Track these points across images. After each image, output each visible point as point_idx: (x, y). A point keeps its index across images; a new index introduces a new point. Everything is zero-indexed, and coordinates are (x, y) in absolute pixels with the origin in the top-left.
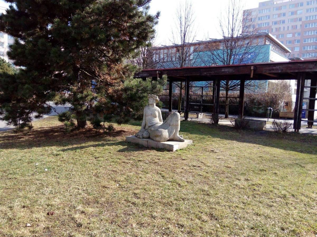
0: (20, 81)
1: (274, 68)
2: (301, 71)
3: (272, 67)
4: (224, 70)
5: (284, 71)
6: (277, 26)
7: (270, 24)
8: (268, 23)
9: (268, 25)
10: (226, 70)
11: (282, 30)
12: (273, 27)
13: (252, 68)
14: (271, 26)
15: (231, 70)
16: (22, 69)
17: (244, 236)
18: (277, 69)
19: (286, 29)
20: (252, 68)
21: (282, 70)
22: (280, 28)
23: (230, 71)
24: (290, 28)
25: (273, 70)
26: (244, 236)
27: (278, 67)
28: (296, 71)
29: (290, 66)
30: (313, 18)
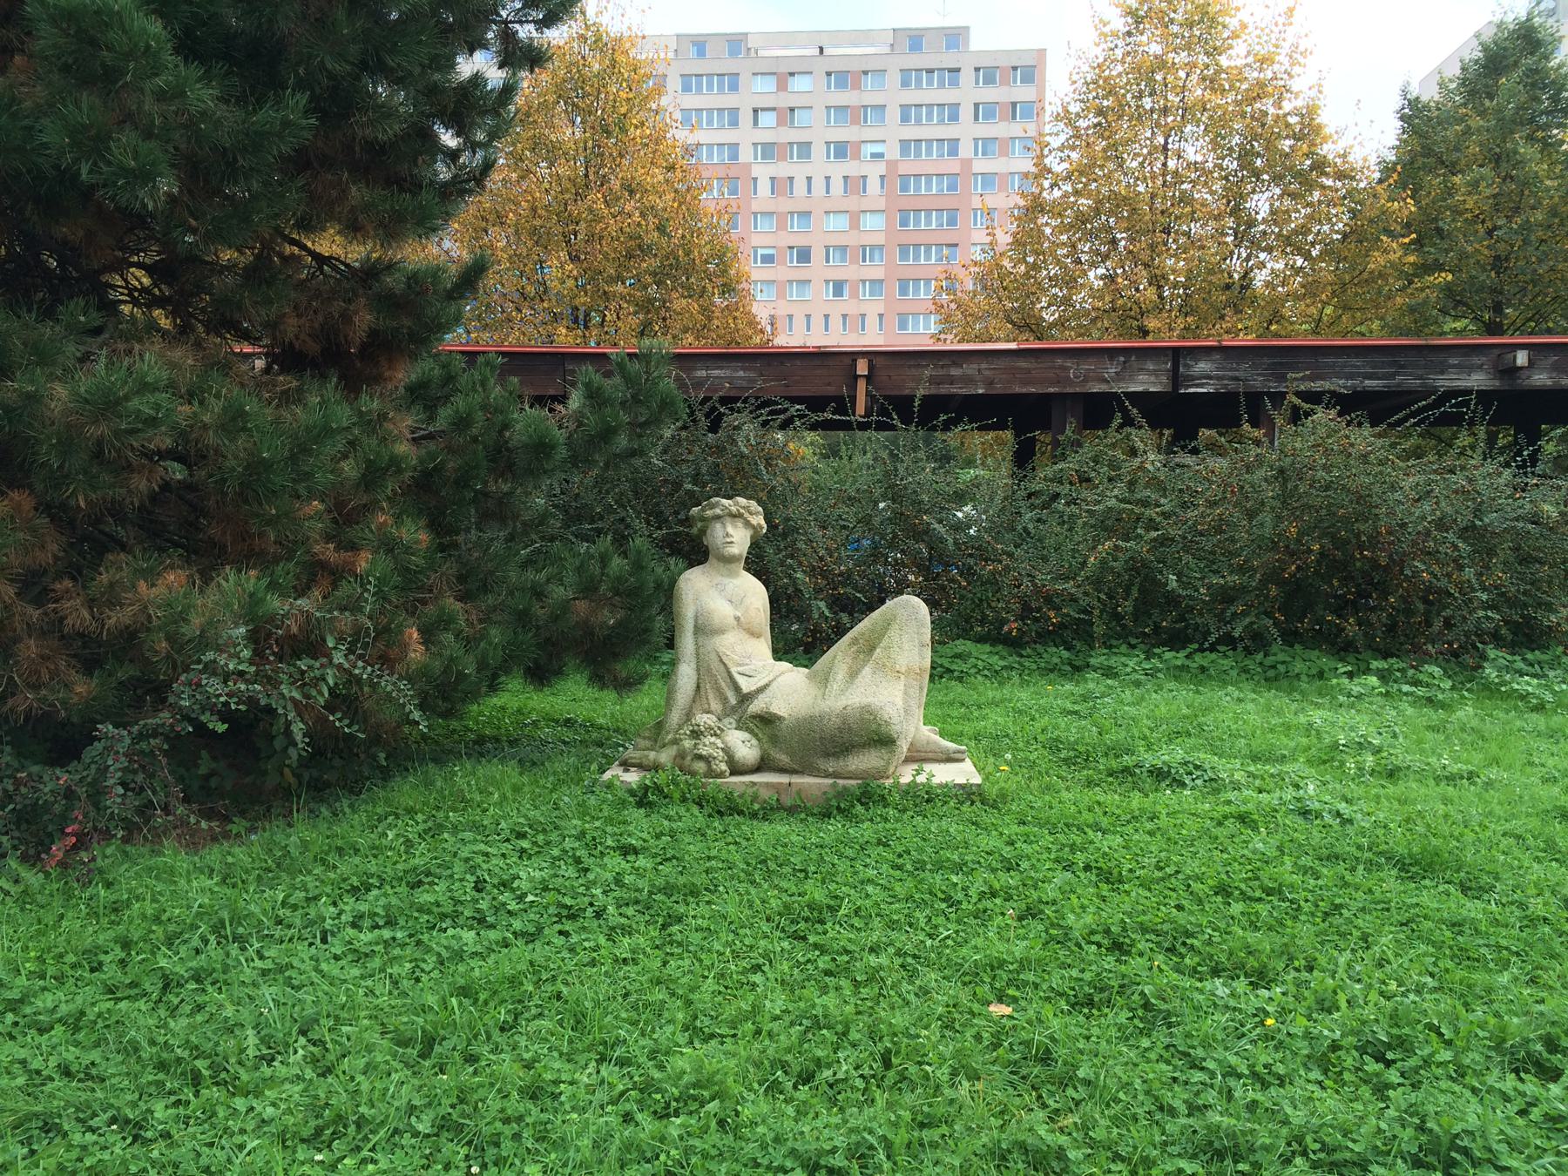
0: (1545, 1055)
1: (955, 372)
2: (1069, 390)
3: (942, 367)
4: (703, 373)
5: (999, 389)
6: (782, 169)
7: (745, 155)
8: (734, 147)
9: (734, 155)
10: (716, 372)
11: (800, 188)
12: (757, 171)
13: (862, 368)
14: (748, 166)
15: (741, 373)
16: (414, 357)
17: (812, 1168)
18: (968, 380)
19: (819, 186)
20: (862, 368)
21: (991, 383)
22: (791, 179)
23: (741, 378)
24: (837, 187)
25: (952, 380)
26: (812, 1168)
27: (970, 369)
28: (1052, 390)
29: (1023, 364)
30: (710, 155)
